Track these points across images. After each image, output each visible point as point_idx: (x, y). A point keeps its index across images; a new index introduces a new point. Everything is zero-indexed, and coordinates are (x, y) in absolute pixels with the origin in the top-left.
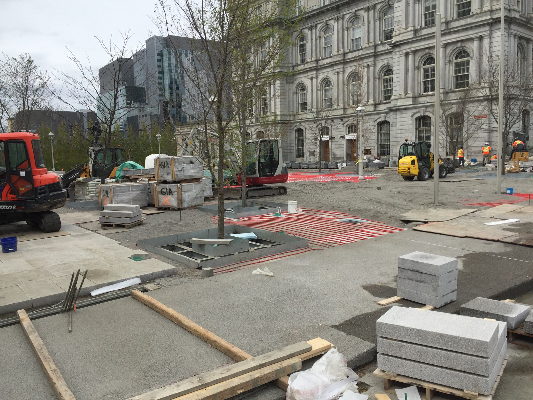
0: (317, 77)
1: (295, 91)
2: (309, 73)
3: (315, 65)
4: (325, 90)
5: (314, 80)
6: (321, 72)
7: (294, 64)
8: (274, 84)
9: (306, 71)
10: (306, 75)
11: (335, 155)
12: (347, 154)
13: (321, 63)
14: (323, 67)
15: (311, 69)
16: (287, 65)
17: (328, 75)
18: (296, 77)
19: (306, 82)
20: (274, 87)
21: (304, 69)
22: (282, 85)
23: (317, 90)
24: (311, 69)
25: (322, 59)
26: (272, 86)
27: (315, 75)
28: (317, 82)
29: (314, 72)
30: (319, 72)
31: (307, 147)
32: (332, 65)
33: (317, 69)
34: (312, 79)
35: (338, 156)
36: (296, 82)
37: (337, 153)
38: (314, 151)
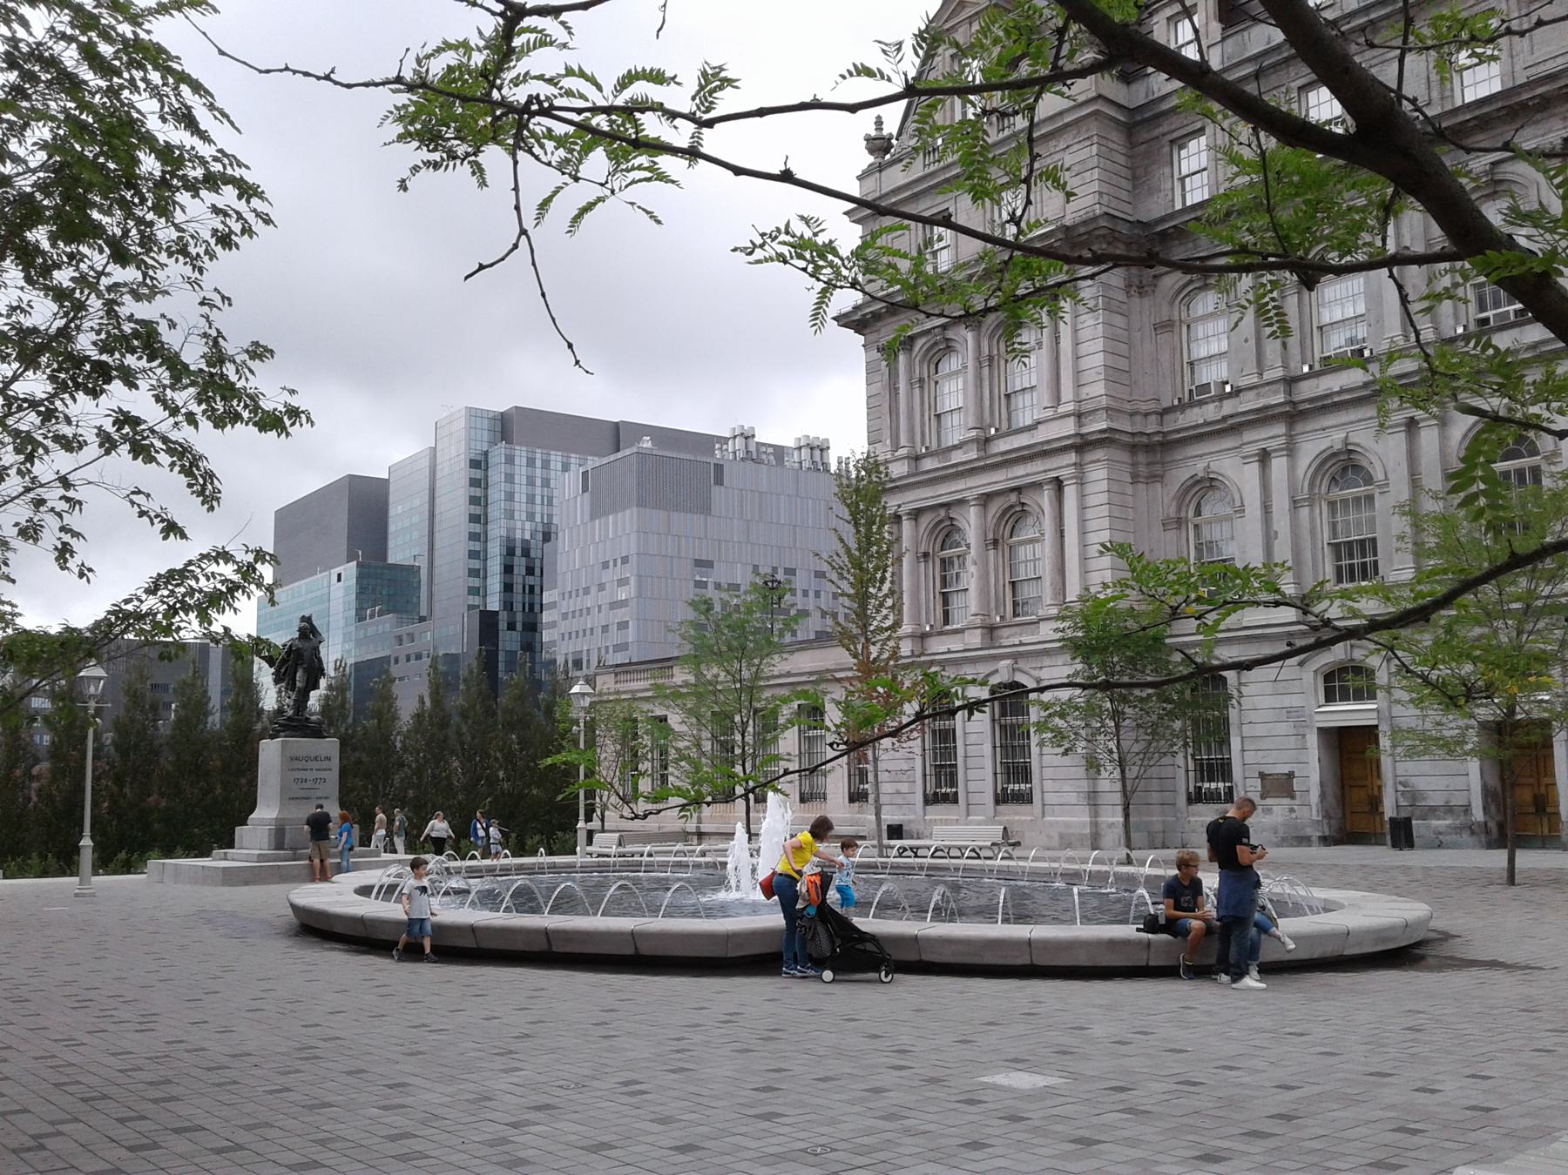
0: (1291, 450)
1: (1172, 512)
2: (1249, 436)
3: (1280, 398)
4: (1332, 504)
5: (1278, 464)
6: (1310, 425)
7: (1166, 404)
8: (1081, 482)
9: (1231, 427)
10: (1228, 442)
11: (1414, 796)
12: (1487, 792)
13: (1307, 390)
14: (1326, 406)
15: (1263, 417)
16: (1128, 407)
17: (1354, 438)
18: (1179, 454)
19: (1229, 473)
20: (1082, 496)
21: (1225, 419)
22: (1115, 488)
23: (1295, 504)
24: (1263, 417)
25: (1313, 375)
26: (1070, 492)
27: (1282, 440)
28: (1292, 469)
29: (1279, 429)
30: (1299, 428)
31: (1250, 757)
32: (1371, 395)
33: (1294, 414)
34: (1264, 457)
35: (1436, 800)
36: (1180, 475)
37: (1421, 784)
38: (1291, 775)
